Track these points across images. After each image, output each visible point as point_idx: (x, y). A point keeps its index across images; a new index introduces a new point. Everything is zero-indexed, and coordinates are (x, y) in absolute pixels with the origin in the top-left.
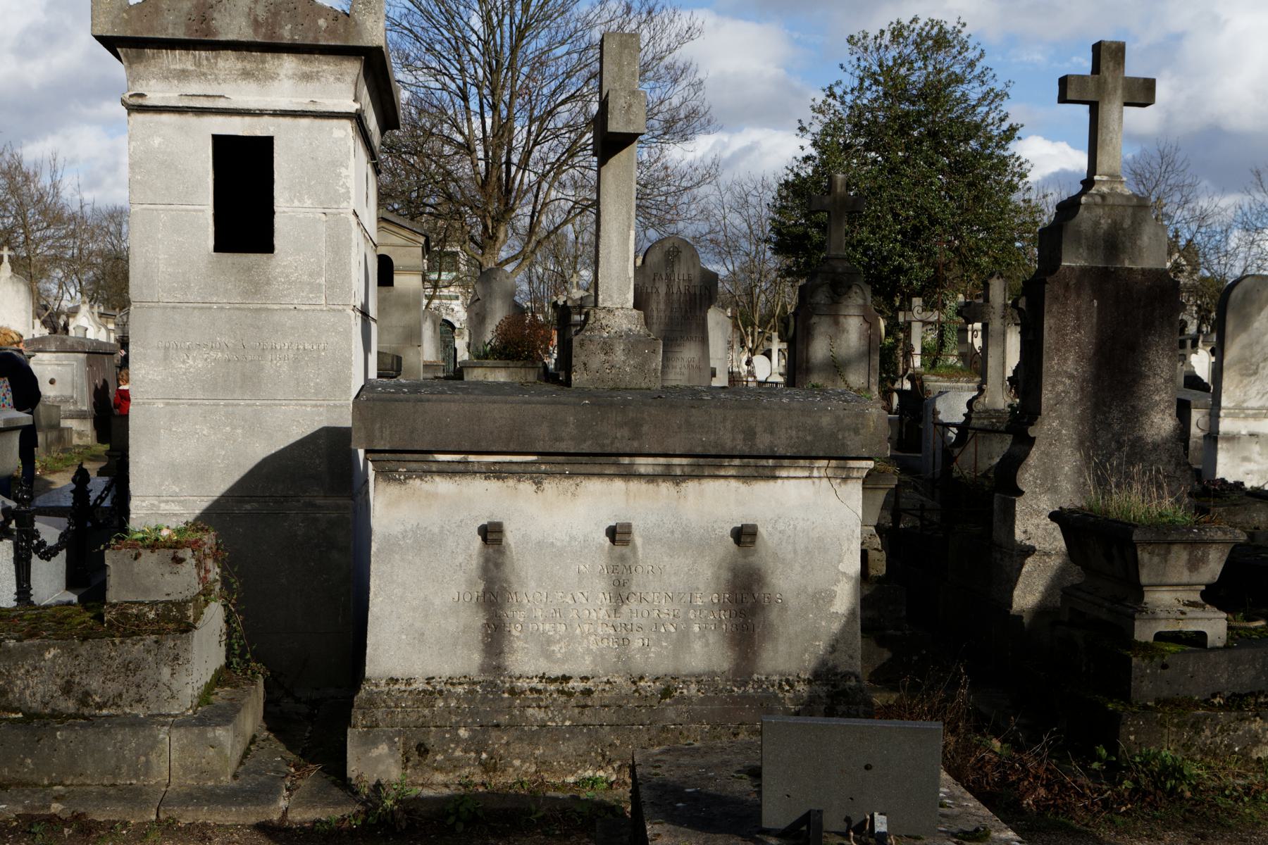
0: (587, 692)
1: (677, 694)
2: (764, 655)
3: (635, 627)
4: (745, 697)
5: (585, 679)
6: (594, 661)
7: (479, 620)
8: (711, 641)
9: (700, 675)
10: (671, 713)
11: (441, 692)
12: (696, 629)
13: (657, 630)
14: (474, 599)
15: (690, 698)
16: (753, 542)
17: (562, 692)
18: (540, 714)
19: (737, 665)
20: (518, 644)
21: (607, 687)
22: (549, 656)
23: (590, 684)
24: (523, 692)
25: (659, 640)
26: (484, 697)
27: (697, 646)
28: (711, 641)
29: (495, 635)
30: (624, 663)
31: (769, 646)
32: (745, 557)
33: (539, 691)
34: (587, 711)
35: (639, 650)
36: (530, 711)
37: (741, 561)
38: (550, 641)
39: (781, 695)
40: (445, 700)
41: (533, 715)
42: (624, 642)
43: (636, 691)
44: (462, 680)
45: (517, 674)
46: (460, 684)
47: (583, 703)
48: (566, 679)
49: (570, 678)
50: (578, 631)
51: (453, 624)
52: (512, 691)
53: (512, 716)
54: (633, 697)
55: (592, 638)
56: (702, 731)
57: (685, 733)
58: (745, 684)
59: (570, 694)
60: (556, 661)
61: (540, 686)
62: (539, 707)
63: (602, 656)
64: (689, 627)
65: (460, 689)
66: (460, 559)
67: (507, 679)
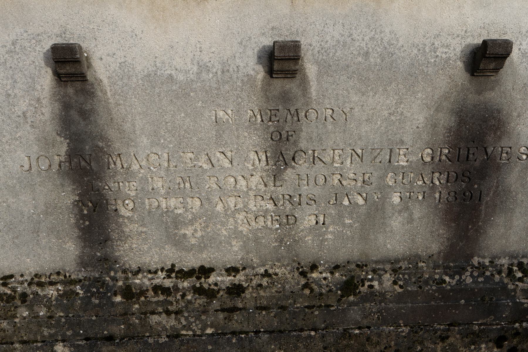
0: (236, 290)
1: (364, 289)
2: (491, 232)
3: (304, 200)
4: (460, 290)
5: (232, 270)
6: (244, 247)
7: (68, 197)
8: (417, 215)
9: (397, 261)
10: (355, 314)
11: (24, 296)
12: (396, 199)
13: (338, 203)
14: (55, 168)
15: (382, 295)
16: (497, 70)
17: (199, 291)
18: (171, 322)
19: (452, 246)
20: (131, 228)
21: (265, 282)
22: (179, 242)
23: (240, 278)
24: (143, 292)
25: (340, 216)
26: (86, 301)
27: (396, 223)
28: (417, 215)
29: (95, 217)
30: (289, 248)
31: (499, 220)
32: (479, 92)
33: (166, 291)
34: (236, 316)
35: (311, 229)
36: (155, 318)
37: (472, 98)
38: (178, 222)
39: (511, 287)
40: (30, 308)
41: (159, 323)
42: (288, 220)
43: (306, 286)
44: (54, 277)
45: (134, 267)
46: (52, 283)
47: (229, 304)
48: (205, 271)
49: (211, 270)
50: (220, 207)
51: (27, 204)
52: (129, 293)
53: (129, 326)
54: (302, 296)
55: (241, 216)
56: (398, 335)
57: (375, 339)
58: (461, 270)
59: (210, 294)
60: (189, 249)
61: (168, 283)
62: (168, 313)
63: (256, 240)
64: (384, 198)
65: (52, 292)
66: (23, 105)
67: (120, 274)
